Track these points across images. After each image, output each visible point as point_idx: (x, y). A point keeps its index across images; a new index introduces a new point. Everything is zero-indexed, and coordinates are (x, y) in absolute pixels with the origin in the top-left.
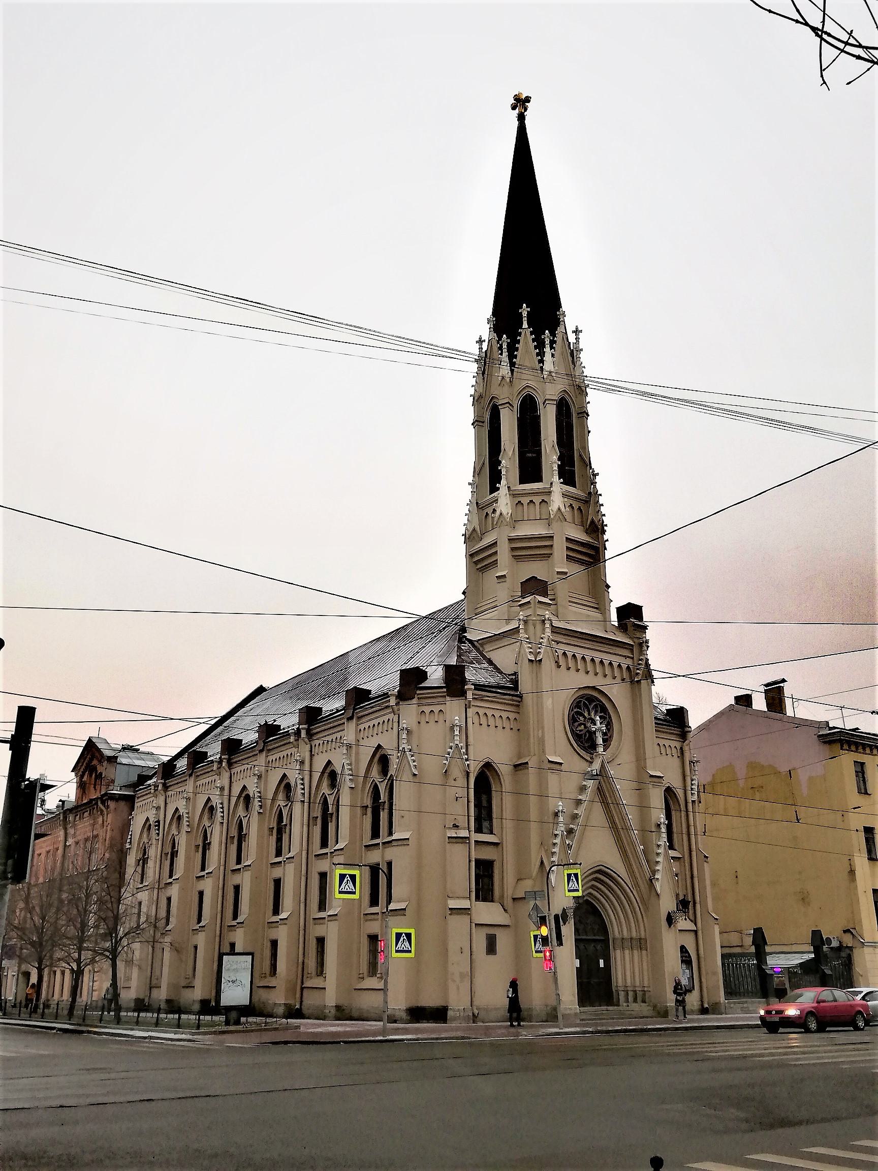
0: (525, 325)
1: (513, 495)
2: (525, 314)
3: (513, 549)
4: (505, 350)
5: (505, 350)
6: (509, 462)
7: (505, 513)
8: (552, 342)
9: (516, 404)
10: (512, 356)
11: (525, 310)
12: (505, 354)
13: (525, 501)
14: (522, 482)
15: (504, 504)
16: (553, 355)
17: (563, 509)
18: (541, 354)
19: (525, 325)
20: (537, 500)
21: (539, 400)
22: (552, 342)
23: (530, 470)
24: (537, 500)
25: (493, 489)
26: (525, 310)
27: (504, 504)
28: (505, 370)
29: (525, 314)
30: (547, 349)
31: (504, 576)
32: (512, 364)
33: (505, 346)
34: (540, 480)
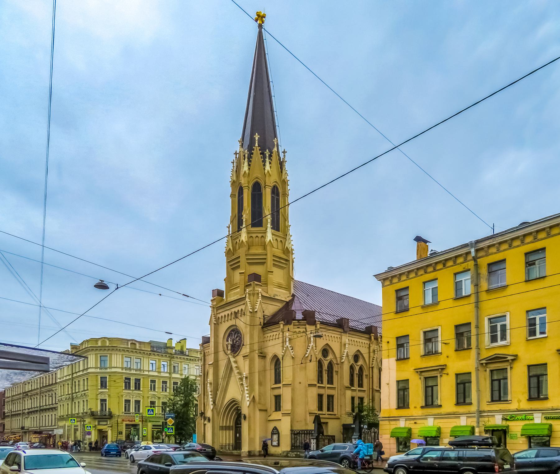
0: (257, 145)
1: (248, 233)
2: (257, 139)
3: (247, 259)
4: (246, 158)
5: (246, 158)
6: (247, 215)
7: (244, 241)
8: (270, 156)
9: (250, 186)
10: (249, 161)
11: (257, 137)
12: (246, 160)
13: (254, 235)
14: (253, 225)
15: (244, 236)
16: (270, 163)
17: (272, 240)
18: (264, 161)
19: (257, 145)
20: (260, 235)
21: (263, 185)
22: (270, 156)
23: (257, 220)
24: (260, 235)
25: (239, 229)
26: (257, 137)
27: (244, 236)
28: (245, 168)
29: (257, 139)
30: (267, 159)
31: (243, 273)
32: (249, 165)
33: (246, 156)
34: (262, 226)
